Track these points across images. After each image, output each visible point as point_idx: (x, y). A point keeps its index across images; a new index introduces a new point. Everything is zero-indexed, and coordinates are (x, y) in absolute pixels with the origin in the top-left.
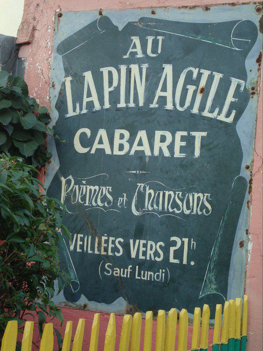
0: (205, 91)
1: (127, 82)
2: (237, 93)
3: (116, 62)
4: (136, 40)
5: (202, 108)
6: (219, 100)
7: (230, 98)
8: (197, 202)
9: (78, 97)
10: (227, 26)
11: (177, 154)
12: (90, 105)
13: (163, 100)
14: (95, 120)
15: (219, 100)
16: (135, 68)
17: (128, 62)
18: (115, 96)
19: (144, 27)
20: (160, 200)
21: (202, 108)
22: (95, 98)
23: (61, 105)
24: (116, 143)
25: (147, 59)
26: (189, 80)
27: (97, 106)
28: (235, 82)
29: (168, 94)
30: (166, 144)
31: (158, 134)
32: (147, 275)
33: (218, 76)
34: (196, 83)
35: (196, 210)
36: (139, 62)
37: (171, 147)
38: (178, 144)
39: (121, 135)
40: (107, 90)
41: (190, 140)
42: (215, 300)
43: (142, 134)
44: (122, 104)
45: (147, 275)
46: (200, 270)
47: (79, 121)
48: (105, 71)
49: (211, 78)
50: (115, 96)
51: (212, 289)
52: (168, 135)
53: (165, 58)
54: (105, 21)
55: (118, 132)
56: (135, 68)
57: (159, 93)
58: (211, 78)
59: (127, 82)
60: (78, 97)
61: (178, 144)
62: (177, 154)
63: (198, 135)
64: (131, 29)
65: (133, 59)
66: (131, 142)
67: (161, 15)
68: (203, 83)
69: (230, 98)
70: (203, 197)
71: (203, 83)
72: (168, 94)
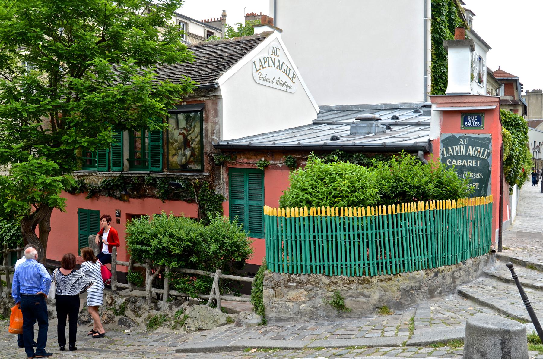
0: (480, 152)
2: (487, 152)
4: (462, 140)
5: (479, 155)
6: (483, 154)
7: (486, 154)
8: (479, 176)
9: (447, 152)
10: (485, 138)
11: (474, 165)
12: (451, 154)
13: (469, 154)
14: (452, 157)
15: (483, 154)
16: (462, 146)
17: (460, 145)
18: (457, 152)
19: (464, 138)
21: (479, 155)
22: (452, 153)
23: (443, 154)
25: (465, 144)
26: (476, 149)
27: (452, 154)
28: (487, 150)
29: (471, 152)
31: (469, 161)
33: (483, 149)
34: (477, 150)
35: (479, 177)
36: (463, 145)
37: (472, 164)
38: (474, 163)
39: (459, 161)
40: (455, 151)
41: (477, 162)
42: (485, 196)
43: (465, 161)
44: (459, 154)
46: (481, 190)
48: (454, 147)
49: (481, 149)
50: (457, 152)
51: (484, 193)
52: (471, 161)
53: (469, 144)
54: (453, 136)
55: (458, 160)
56: (462, 146)
57: (468, 152)
58: (481, 149)
61: (474, 163)
62: (474, 165)
63: (479, 161)
64: (460, 138)
65: (461, 144)
66: (462, 162)
67: (468, 135)
68: (479, 150)
69: (486, 154)
70: (481, 174)
71: (479, 150)
72: (471, 152)
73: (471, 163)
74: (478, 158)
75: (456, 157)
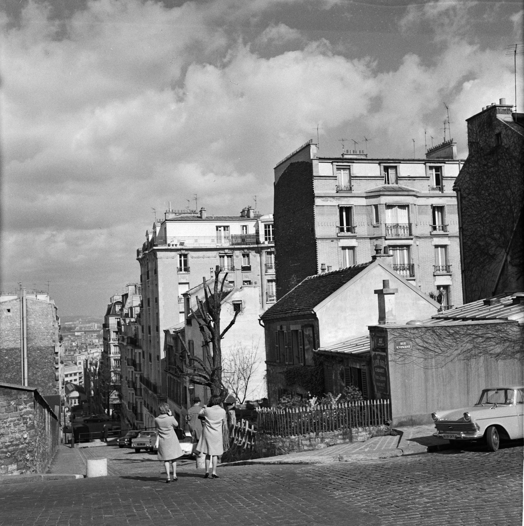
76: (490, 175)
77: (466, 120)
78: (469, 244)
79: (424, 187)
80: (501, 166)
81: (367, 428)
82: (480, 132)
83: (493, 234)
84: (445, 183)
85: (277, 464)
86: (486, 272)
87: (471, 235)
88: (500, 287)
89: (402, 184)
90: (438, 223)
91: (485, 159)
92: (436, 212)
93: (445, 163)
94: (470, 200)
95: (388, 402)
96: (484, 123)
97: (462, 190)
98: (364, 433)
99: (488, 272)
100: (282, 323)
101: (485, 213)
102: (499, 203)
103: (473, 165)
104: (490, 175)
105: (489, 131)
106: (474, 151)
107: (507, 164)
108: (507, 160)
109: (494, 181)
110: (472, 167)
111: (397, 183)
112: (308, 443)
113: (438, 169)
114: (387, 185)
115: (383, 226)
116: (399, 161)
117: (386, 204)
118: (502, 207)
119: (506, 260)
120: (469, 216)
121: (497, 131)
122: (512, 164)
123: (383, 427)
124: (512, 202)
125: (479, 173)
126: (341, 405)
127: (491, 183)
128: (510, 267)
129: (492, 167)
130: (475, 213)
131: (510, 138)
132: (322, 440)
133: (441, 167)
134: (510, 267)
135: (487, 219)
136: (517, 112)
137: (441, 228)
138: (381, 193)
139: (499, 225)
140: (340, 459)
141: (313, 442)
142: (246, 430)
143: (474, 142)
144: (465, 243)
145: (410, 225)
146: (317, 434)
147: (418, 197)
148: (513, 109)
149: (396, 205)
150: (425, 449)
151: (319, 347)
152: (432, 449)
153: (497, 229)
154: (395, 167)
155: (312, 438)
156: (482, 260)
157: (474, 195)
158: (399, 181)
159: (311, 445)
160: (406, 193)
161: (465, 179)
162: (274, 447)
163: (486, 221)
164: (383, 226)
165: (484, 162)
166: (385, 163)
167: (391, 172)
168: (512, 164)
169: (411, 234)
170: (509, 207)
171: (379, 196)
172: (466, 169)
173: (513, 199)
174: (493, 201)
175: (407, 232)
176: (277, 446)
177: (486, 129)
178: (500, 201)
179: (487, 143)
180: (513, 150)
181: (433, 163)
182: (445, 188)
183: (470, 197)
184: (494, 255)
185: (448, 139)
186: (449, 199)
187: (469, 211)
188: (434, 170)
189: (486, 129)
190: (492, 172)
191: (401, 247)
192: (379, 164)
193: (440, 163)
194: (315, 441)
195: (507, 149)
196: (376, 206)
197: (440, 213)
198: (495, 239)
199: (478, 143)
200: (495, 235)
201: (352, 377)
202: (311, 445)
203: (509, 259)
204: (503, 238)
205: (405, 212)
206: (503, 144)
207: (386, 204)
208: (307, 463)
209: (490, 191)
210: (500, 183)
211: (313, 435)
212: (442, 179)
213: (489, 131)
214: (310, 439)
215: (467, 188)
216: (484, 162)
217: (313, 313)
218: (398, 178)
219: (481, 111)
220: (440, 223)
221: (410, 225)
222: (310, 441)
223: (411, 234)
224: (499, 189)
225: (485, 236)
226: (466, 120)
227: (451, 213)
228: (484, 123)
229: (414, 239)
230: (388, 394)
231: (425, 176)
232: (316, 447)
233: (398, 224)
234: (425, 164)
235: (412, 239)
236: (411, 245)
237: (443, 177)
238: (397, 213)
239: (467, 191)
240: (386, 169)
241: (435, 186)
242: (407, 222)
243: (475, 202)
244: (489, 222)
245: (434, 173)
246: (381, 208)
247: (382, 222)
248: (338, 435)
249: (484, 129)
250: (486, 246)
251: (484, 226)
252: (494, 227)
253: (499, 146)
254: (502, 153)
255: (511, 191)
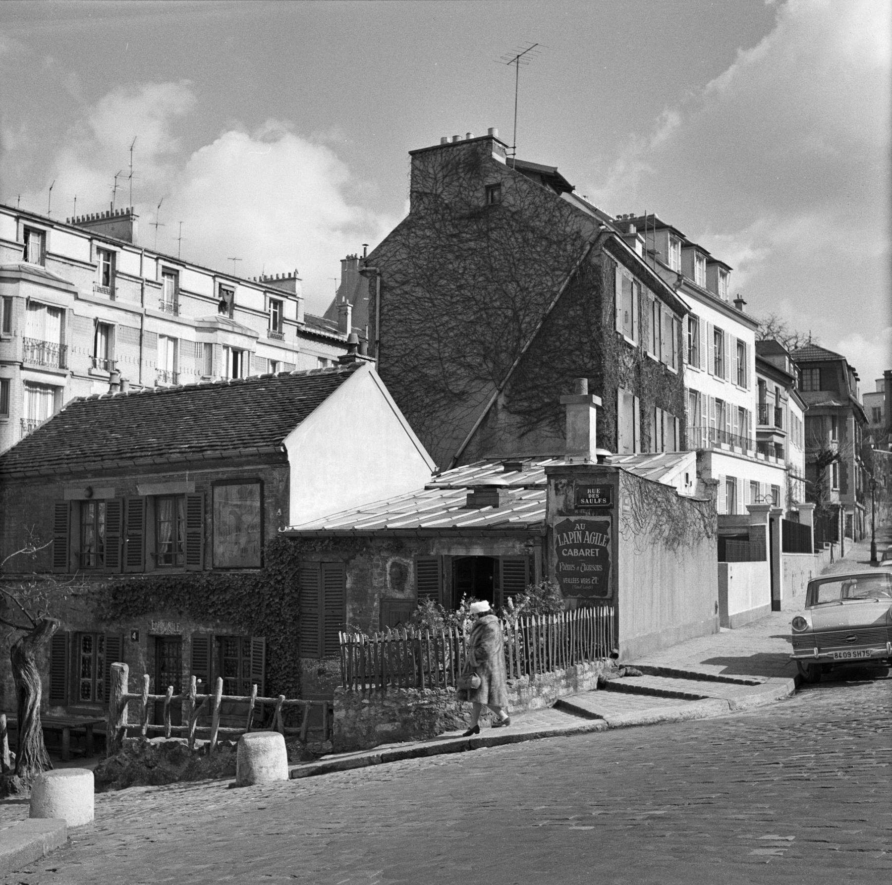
1: (575, 536)
3: (572, 530)
6: (602, 540)
8: (598, 568)
9: (562, 539)
14: (567, 547)
15: (602, 540)
18: (573, 540)
19: (579, 522)
20: (588, 568)
24: (575, 553)
30: (589, 552)
32: (586, 587)
45: (586, 587)
47: (563, 547)
50: (573, 540)
59: (575, 536)
60: (562, 539)
64: (576, 522)
70: (600, 566)
73: (589, 552)
74: (597, 547)
75: (573, 546)
76: (465, 254)
77: (411, 153)
78: (396, 373)
79: (88, 282)
80: (496, 241)
81: (593, 663)
82: (445, 177)
83: (464, 357)
84: (118, 282)
85: (603, 730)
86: (435, 423)
87: (403, 356)
88: (472, 448)
89: (52, 268)
90: (101, 354)
91: (455, 226)
92: (99, 334)
93: (121, 247)
94: (406, 293)
95: (612, 614)
96: (458, 163)
97: (385, 276)
98: (590, 674)
99: (443, 422)
100: (91, 481)
101: (446, 318)
102: (485, 303)
103: (419, 233)
104: (465, 254)
105: (470, 179)
106: (426, 209)
107: (513, 239)
108: (513, 232)
109: (476, 265)
110: (417, 236)
111: (43, 264)
112: (515, 697)
113: (110, 256)
114: (24, 263)
115: (19, 341)
116: (51, 224)
117: (28, 300)
118: (490, 312)
119: (495, 403)
120: (401, 321)
121: (490, 181)
122: (525, 240)
123: (609, 661)
124: (518, 304)
125: (436, 248)
126: (537, 621)
127: (465, 268)
128: (502, 416)
129: (471, 240)
130: (417, 317)
131: (523, 195)
132: (540, 686)
133: (114, 253)
134: (502, 416)
135: (452, 329)
136: (516, 157)
137: (102, 365)
138: (23, 276)
139: (482, 343)
140: (731, 705)
141: (525, 696)
142: (219, 700)
143: (426, 194)
144: (385, 369)
145: (63, 348)
146: (532, 679)
147: (77, 298)
148: (510, 151)
149: (45, 306)
150: (789, 684)
151: (288, 524)
152: (802, 684)
153: (475, 348)
154: (42, 234)
155: (523, 687)
156: (427, 401)
157: (418, 285)
158: (47, 262)
159: (520, 702)
160: (63, 286)
161: (394, 256)
162: (431, 714)
163: (446, 332)
164: (19, 341)
165: (451, 230)
166: (27, 219)
167: (34, 239)
168: (525, 240)
169: (62, 367)
170: (510, 313)
171: (18, 280)
172: (398, 238)
173: (523, 299)
174: (469, 299)
175: (56, 361)
176: (441, 712)
177: (462, 175)
178: (487, 300)
179: (462, 199)
180: (531, 217)
181: (103, 241)
182: (117, 293)
183: (407, 288)
184: (463, 393)
185: (122, 206)
186: (122, 313)
187: (400, 314)
188: (102, 255)
189: (462, 175)
190: (470, 249)
191: (45, 386)
192: (17, 219)
193: (114, 245)
194: (528, 692)
195: (514, 213)
196: (8, 300)
197: (103, 337)
198: (470, 366)
199: (437, 196)
200: (469, 359)
201: (443, 576)
202: (520, 702)
203: (502, 401)
204: (491, 365)
205: (54, 322)
206: (505, 204)
207: (28, 300)
208: (675, 721)
209: (463, 282)
210: (492, 269)
211: (524, 679)
212: (114, 276)
213: (470, 179)
214: (519, 689)
215: (399, 271)
216: (451, 230)
217: (282, 450)
218: (45, 255)
219: (439, 143)
220: (103, 357)
221: (63, 348)
222: (519, 694)
223: (62, 367)
224: (487, 279)
225: (441, 359)
226: (411, 153)
227: (123, 341)
228: (458, 163)
229: (68, 377)
230: (609, 596)
231: (88, 261)
232: (530, 706)
233: (44, 343)
234: (90, 240)
235: (65, 376)
236: (62, 387)
237: (116, 273)
238: (45, 320)
239: (399, 277)
240: (27, 231)
241: (101, 286)
242: (58, 342)
243: (418, 298)
244: (456, 335)
245: (102, 262)
246: (19, 306)
247: (18, 333)
248: (560, 679)
249: (457, 173)
250: (445, 377)
251: (440, 342)
252: (466, 345)
253: (494, 205)
254: (500, 219)
255: (518, 285)
